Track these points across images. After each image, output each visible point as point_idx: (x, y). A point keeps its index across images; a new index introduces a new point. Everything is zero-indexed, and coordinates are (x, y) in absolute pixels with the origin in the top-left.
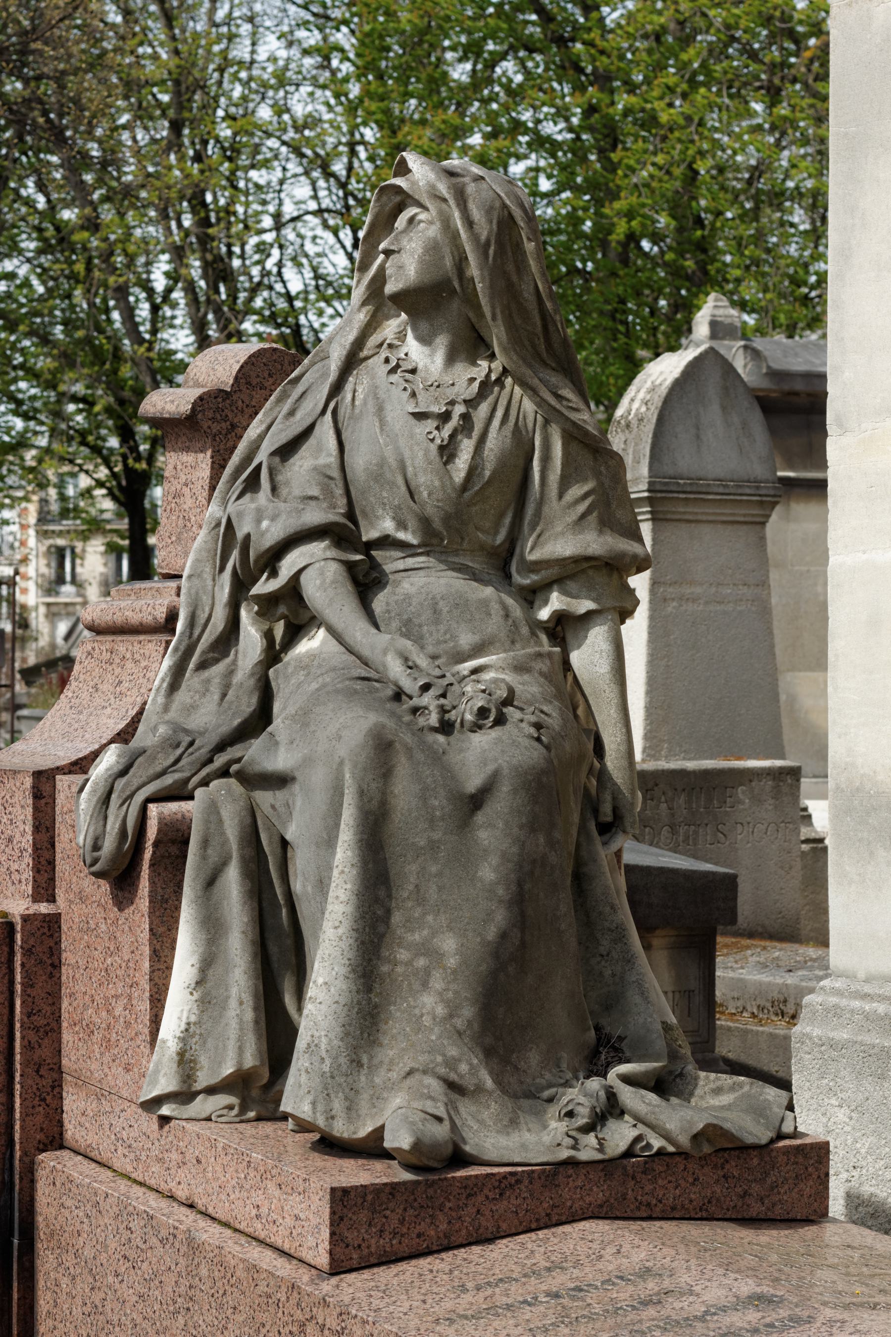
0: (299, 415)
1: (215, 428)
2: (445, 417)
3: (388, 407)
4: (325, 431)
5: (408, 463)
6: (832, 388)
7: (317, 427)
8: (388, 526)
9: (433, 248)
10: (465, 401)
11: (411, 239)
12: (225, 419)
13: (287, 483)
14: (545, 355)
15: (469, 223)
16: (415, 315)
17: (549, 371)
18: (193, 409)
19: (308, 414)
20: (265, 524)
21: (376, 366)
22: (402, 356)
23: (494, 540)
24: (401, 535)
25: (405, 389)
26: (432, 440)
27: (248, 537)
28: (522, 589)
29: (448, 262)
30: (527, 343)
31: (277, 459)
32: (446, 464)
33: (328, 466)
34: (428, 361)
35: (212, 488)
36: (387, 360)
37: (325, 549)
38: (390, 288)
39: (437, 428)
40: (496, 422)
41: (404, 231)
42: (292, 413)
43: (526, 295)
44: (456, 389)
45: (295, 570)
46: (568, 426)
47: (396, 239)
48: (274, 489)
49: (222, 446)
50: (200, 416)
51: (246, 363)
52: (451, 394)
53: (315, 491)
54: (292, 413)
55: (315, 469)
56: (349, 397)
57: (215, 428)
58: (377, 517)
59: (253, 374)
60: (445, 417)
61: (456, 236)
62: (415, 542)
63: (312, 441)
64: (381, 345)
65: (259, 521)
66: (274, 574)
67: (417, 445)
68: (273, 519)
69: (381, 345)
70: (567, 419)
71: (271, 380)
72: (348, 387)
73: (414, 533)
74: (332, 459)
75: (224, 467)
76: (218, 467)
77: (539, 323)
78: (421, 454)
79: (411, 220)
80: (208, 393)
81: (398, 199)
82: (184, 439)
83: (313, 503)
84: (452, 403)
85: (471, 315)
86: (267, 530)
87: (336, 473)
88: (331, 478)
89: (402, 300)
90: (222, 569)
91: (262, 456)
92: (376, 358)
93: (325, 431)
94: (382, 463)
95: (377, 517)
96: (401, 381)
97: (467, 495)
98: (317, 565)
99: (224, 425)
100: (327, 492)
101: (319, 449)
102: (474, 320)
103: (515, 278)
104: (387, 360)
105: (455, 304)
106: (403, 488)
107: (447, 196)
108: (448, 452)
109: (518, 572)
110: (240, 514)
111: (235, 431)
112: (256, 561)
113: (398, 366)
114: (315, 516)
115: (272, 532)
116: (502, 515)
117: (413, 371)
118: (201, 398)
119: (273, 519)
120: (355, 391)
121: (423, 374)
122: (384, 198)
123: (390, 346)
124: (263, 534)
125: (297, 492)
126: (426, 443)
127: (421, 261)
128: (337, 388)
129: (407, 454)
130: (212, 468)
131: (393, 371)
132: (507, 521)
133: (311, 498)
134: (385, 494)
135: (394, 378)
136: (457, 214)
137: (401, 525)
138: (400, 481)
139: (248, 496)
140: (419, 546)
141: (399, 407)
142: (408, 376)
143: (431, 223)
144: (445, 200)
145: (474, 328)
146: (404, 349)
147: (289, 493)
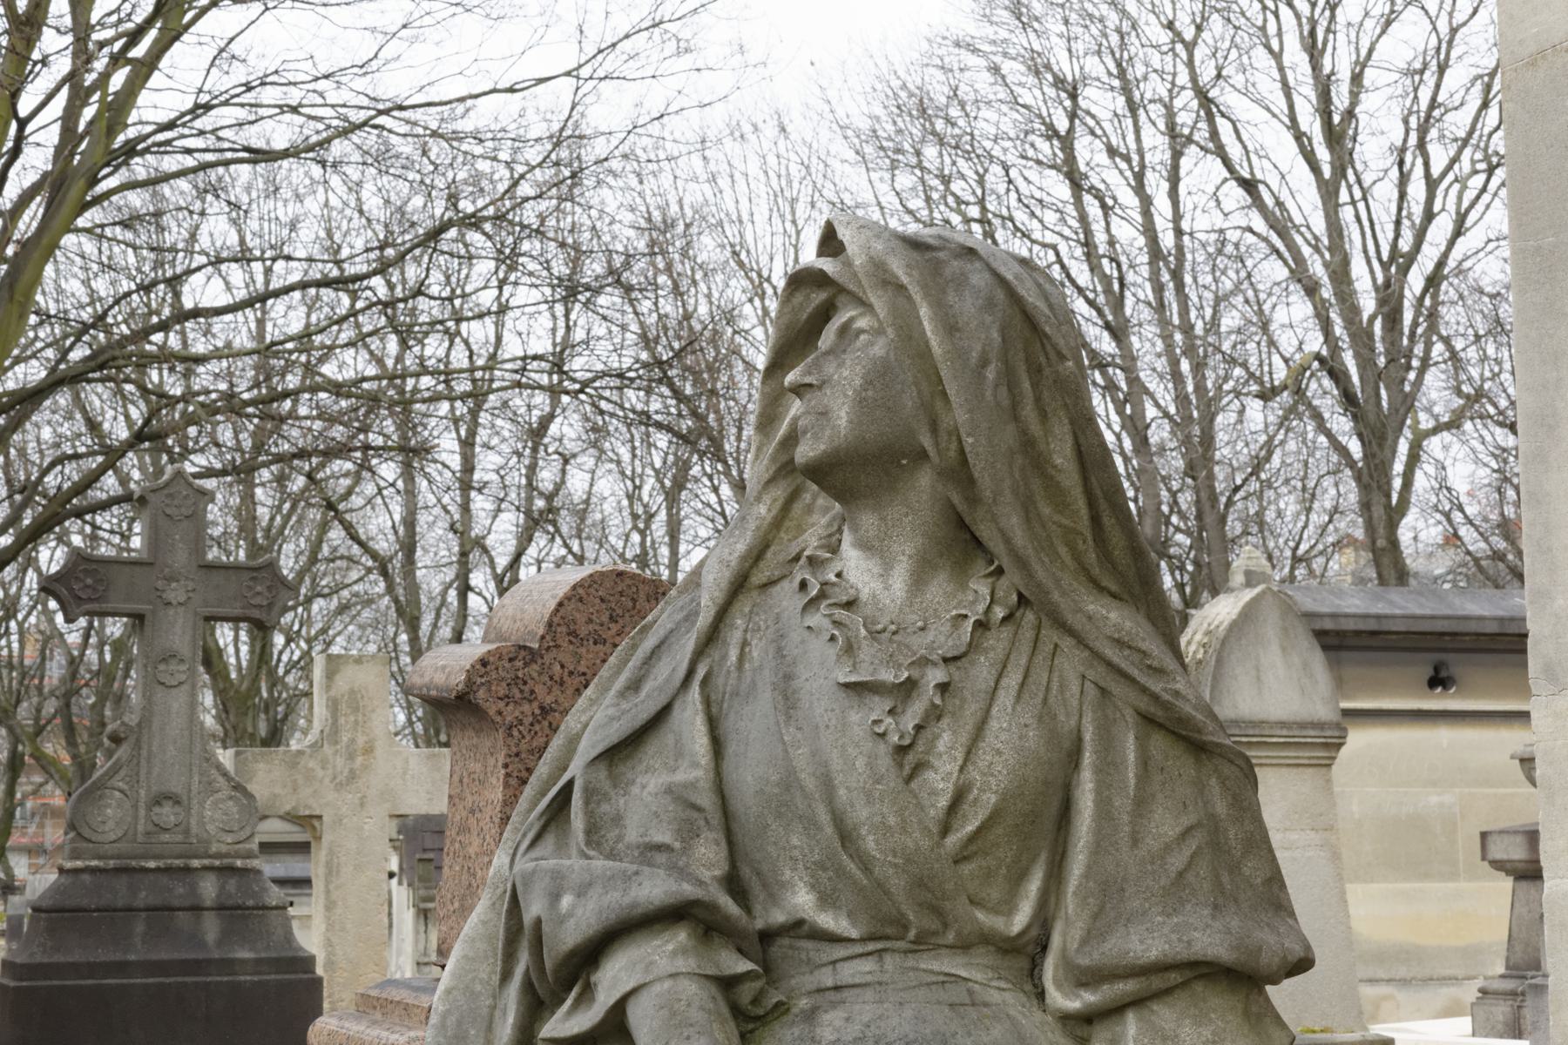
0: (647, 687)
1: (511, 713)
2: (909, 688)
3: (803, 673)
4: (690, 722)
5: (839, 779)
6: (1529, 625)
7: (676, 711)
8: (802, 901)
9: (880, 375)
10: (946, 660)
11: (841, 365)
12: (531, 697)
13: (618, 820)
14: (1096, 571)
15: (950, 328)
16: (844, 495)
17: (1107, 600)
18: (469, 682)
19: (660, 689)
20: (566, 901)
21: (786, 598)
22: (832, 577)
23: (1009, 923)
24: (827, 921)
25: (833, 638)
26: (883, 735)
27: (538, 922)
28: (1066, 1018)
29: (909, 402)
30: (1063, 550)
31: (602, 773)
32: (909, 779)
33: (692, 785)
34: (877, 585)
35: (505, 820)
36: (803, 585)
37: (674, 953)
38: (805, 452)
39: (891, 712)
40: (1005, 699)
41: (827, 353)
42: (635, 686)
43: (1059, 461)
44: (930, 636)
45: (617, 995)
46: (1144, 704)
47: (817, 365)
48: (593, 832)
49: (524, 746)
50: (481, 694)
51: (568, 598)
52: (920, 644)
53: (662, 836)
54: (635, 686)
55: (669, 790)
56: (733, 655)
57: (511, 713)
58: (783, 885)
59: (581, 618)
60: (909, 688)
61: (925, 353)
62: (854, 934)
63: (664, 739)
64: (797, 558)
65: (555, 897)
66: (588, 993)
67: (849, 744)
68: (581, 893)
69: (797, 558)
70: (1144, 690)
71: (614, 628)
72: (734, 637)
73: (850, 915)
74: (700, 773)
75: (524, 782)
76: (517, 780)
77: (1084, 512)
78: (860, 763)
79: (844, 330)
80: (498, 653)
81: (819, 297)
82: (471, 733)
83: (661, 858)
84: (924, 662)
85: (956, 499)
86: (570, 914)
87: (706, 800)
88: (699, 809)
89: (823, 473)
90: (506, 976)
91: (575, 769)
92: (785, 584)
93: (690, 722)
94: (789, 781)
95: (783, 885)
96: (826, 623)
97: (953, 840)
98: (657, 988)
99: (526, 707)
100: (689, 833)
101: (679, 754)
102: (962, 507)
103: (1035, 429)
104: (803, 585)
105: (925, 480)
106: (829, 830)
107: (905, 280)
108: (908, 757)
109: (1059, 986)
110: (528, 878)
111: (549, 717)
112: (556, 971)
113: (823, 595)
114: (655, 889)
115: (576, 920)
116: (1018, 878)
117: (850, 605)
118: (484, 662)
119: (581, 893)
120: (745, 644)
121: (868, 611)
122: (799, 298)
123: (813, 562)
124: (562, 920)
125: (632, 835)
126: (868, 745)
127: (861, 402)
128: (712, 637)
129: (836, 764)
130: (506, 785)
131: (813, 603)
132: (1034, 885)
133: (659, 847)
134: (795, 841)
135: (816, 619)
136: (924, 311)
137: (826, 900)
138: (824, 817)
139: (549, 840)
140: (863, 940)
141: (821, 669)
142: (841, 614)
143: (880, 331)
144: (901, 288)
145: (961, 524)
146: (837, 566)
147: (620, 838)
